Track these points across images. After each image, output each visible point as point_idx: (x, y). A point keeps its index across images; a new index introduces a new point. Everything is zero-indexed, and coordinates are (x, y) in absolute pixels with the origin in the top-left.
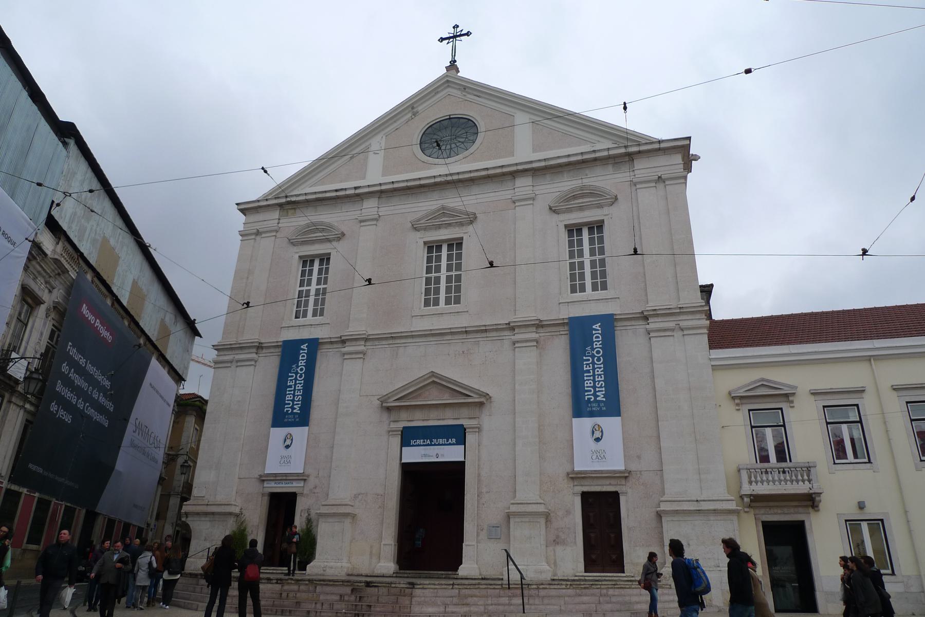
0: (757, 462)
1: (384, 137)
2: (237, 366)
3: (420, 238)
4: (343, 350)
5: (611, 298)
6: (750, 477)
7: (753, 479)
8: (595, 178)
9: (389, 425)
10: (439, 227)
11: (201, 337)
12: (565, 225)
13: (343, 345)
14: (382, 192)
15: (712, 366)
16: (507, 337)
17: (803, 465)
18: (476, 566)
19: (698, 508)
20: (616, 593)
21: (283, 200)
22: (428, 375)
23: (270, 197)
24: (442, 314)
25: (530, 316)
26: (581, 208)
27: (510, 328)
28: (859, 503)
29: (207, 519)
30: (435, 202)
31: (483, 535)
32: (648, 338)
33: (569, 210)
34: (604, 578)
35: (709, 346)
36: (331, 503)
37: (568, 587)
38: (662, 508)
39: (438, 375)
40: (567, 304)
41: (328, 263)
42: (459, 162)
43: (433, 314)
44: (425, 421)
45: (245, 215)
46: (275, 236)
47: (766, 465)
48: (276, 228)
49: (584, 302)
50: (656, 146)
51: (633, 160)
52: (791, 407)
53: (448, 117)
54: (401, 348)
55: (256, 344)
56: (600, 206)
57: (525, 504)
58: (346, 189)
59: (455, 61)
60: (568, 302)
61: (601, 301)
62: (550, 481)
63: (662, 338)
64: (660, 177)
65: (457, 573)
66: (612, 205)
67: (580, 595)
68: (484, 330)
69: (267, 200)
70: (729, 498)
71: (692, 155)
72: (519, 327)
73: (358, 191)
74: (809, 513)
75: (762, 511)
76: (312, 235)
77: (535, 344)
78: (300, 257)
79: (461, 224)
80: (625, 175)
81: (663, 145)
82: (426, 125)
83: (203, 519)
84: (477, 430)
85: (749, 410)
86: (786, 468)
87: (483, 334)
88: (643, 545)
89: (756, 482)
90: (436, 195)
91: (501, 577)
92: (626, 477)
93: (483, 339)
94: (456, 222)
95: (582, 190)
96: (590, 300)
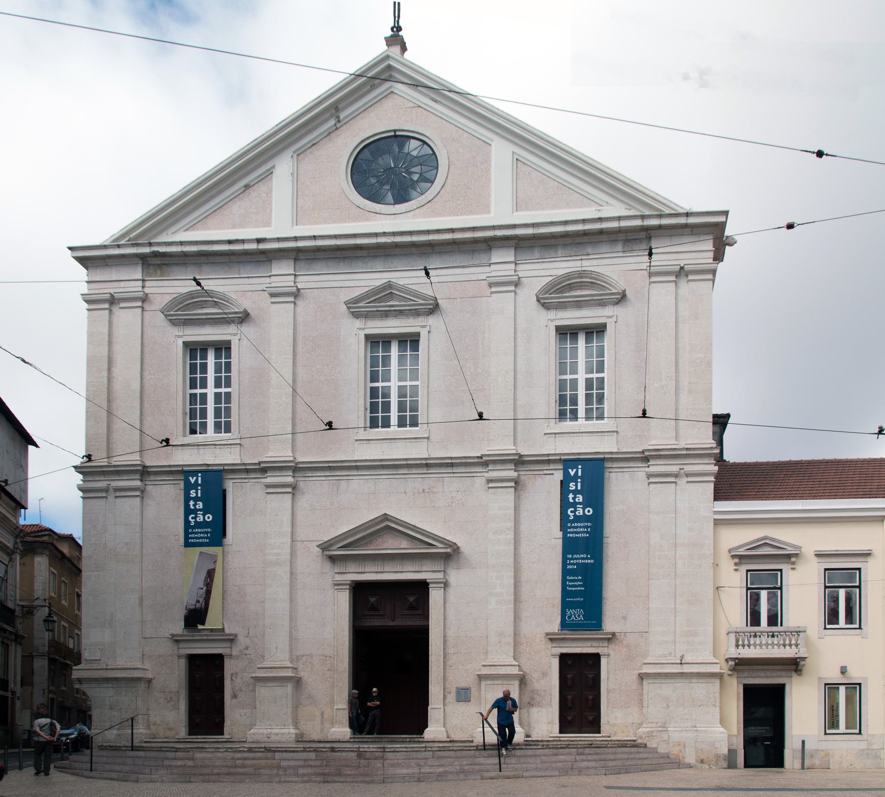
0: (747, 626)
1: (295, 156)
2: (116, 497)
3: (360, 329)
4: (263, 480)
5: (608, 432)
6: (737, 641)
7: (740, 642)
8: (599, 260)
9: (333, 578)
10: (386, 315)
11: (37, 446)
12: (556, 326)
13: (262, 475)
14: (298, 250)
15: (715, 520)
16: (478, 474)
17: (793, 630)
18: (444, 729)
19: (681, 671)
20: (592, 752)
21: (146, 250)
22: (380, 519)
23: (122, 242)
24: (395, 439)
25: (508, 448)
26: (578, 304)
27: (482, 462)
28: (842, 667)
29: (110, 685)
30: (378, 275)
31: (451, 697)
32: (647, 483)
33: (562, 306)
34: (579, 739)
35: (715, 496)
36: (268, 666)
37: (544, 747)
38: (644, 671)
39: (393, 519)
40: (554, 436)
41: (229, 356)
42: (412, 213)
43: (383, 439)
44: (379, 574)
45: (87, 268)
46: (143, 308)
47: (756, 629)
48: (140, 294)
49: (575, 435)
50: (682, 220)
51: (650, 238)
53: (392, 134)
54: (342, 482)
55: (139, 468)
56: (602, 304)
57: (497, 666)
58: (243, 241)
59: (399, 29)
60: (555, 434)
61: (596, 434)
62: (526, 642)
63: (663, 485)
64: (682, 268)
65: (423, 736)
66: (617, 303)
67: (557, 755)
68: (450, 464)
69: (119, 246)
70: (714, 661)
71: (727, 237)
72: (494, 462)
73: (262, 246)
76: (200, 311)
77: (513, 484)
78: (186, 344)
79: (416, 313)
80: (638, 259)
81: (692, 220)
82: (362, 142)
83: (104, 685)
84: (443, 585)
85: (748, 571)
86: (775, 632)
87: (449, 468)
88: (621, 707)
89: (743, 646)
90: (379, 265)
91: (471, 739)
92: (609, 639)
93: (449, 475)
94: (410, 310)
96: (582, 432)
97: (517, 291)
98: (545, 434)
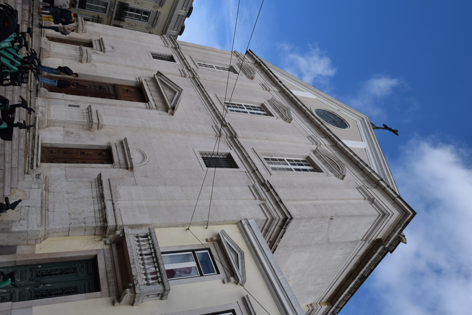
15: (241, 221)
52: (224, 282)
74: (110, 296)
75: (108, 256)
95: (337, 162)
97: (314, 145)
98: (253, 148)
